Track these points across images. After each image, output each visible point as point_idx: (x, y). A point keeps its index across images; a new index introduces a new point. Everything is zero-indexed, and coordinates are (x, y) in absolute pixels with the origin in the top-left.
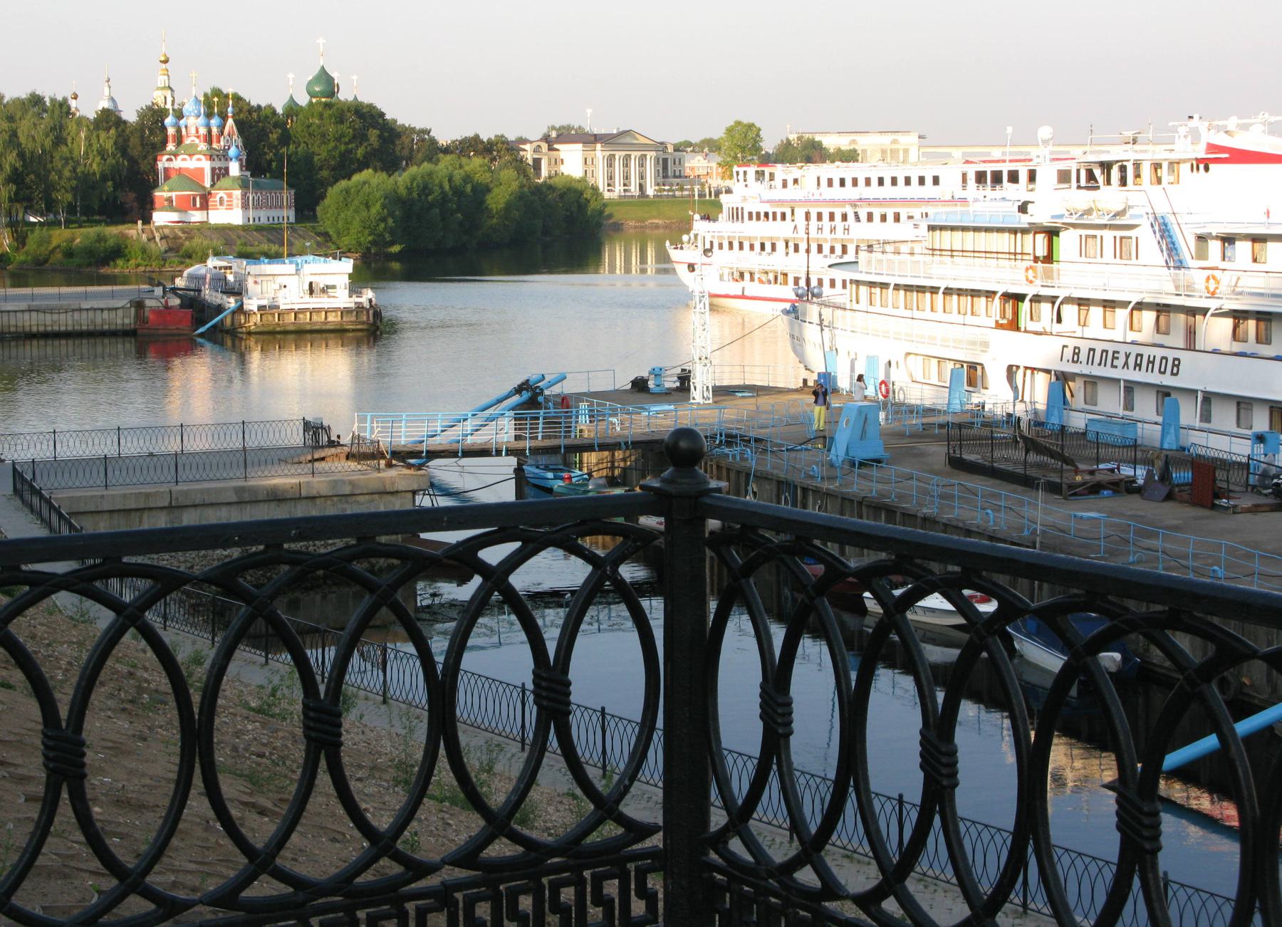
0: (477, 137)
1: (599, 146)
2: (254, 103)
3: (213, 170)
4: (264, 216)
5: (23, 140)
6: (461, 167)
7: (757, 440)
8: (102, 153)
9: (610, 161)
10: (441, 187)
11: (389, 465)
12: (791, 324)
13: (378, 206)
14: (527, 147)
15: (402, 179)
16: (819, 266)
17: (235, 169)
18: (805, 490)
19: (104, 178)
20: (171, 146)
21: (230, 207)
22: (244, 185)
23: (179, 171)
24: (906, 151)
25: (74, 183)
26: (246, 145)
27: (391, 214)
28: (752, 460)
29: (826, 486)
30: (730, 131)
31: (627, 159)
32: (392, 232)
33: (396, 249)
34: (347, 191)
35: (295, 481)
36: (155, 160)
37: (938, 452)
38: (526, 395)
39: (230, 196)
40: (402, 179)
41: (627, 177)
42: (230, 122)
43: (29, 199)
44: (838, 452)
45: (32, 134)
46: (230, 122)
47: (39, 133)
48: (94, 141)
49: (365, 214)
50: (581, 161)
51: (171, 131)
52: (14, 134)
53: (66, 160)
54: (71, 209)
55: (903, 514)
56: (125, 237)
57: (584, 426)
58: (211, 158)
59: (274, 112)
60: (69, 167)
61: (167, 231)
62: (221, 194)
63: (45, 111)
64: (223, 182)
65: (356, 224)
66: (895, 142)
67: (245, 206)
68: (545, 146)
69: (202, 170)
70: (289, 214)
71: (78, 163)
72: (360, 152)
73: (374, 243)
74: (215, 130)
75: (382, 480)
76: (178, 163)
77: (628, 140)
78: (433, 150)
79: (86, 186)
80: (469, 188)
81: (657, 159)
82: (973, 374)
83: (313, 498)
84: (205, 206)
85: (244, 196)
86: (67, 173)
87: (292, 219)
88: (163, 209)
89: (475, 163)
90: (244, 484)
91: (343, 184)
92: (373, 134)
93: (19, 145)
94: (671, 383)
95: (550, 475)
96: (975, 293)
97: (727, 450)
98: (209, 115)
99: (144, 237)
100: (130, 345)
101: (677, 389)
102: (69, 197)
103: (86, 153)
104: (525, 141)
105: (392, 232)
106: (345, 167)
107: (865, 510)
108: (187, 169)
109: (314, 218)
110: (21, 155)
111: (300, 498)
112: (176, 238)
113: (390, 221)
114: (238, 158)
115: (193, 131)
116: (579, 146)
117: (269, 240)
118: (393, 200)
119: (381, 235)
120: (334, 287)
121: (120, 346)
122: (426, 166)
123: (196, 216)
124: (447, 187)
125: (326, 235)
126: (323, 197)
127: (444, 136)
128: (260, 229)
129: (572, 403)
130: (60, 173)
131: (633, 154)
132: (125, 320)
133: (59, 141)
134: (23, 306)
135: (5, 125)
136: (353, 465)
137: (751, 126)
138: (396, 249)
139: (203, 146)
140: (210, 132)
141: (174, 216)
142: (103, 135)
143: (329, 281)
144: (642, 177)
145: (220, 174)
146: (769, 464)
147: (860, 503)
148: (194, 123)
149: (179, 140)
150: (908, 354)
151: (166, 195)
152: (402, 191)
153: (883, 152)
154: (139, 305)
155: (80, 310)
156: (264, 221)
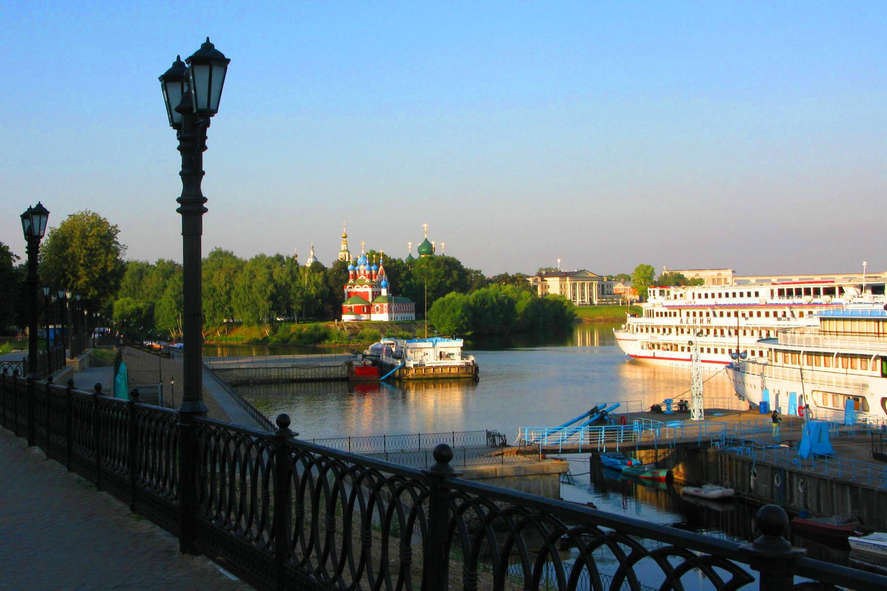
1: (568, 278)
3: (373, 293)
4: (399, 317)
5: (275, 277)
7: (746, 442)
8: (316, 284)
9: (574, 286)
10: (492, 300)
11: (544, 458)
12: (735, 375)
13: (460, 311)
14: (530, 279)
16: (748, 342)
17: (384, 292)
18: (790, 473)
19: (317, 297)
20: (351, 281)
21: (382, 312)
22: (389, 301)
23: (356, 293)
24: (725, 279)
25: (302, 300)
27: (467, 315)
28: (753, 455)
29: (806, 471)
30: (637, 269)
31: (582, 286)
32: (467, 324)
34: (443, 303)
35: (493, 467)
36: (343, 288)
37: (865, 452)
38: (596, 416)
39: (382, 306)
41: (583, 295)
42: (381, 267)
43: (279, 309)
44: (804, 449)
45: (280, 274)
46: (381, 267)
47: (284, 275)
48: (312, 278)
49: (452, 315)
51: (351, 273)
52: (271, 275)
54: (300, 314)
55: (863, 489)
56: (329, 328)
57: (640, 435)
58: (372, 286)
61: (350, 325)
62: (377, 305)
63: (284, 263)
64: (379, 299)
65: (448, 321)
67: (390, 311)
68: (539, 279)
70: (413, 315)
71: (303, 290)
72: (448, 282)
74: (374, 272)
75: (542, 467)
77: (583, 275)
78: (485, 282)
79: (308, 301)
80: (506, 301)
81: (599, 285)
82: (857, 403)
83: (503, 477)
85: (389, 306)
86: (298, 295)
87: (414, 318)
88: (347, 313)
90: (464, 469)
91: (441, 299)
92: (455, 273)
93: (274, 281)
94: (674, 408)
95: (619, 462)
96: (853, 356)
97: (734, 448)
98: (370, 264)
99: (339, 328)
100: (344, 386)
101: (678, 411)
102: (299, 307)
103: (308, 284)
104: (529, 277)
105: (467, 324)
106: (440, 291)
107: (834, 486)
108: (360, 293)
110: (275, 286)
111: (496, 477)
112: (355, 328)
113: (466, 319)
114: (386, 287)
115: (362, 272)
116: (558, 279)
117: (404, 330)
118: (467, 307)
119: (461, 326)
120: (453, 354)
121: (340, 387)
124: (495, 300)
127: (489, 274)
128: (398, 323)
129: (628, 421)
130: (295, 295)
131: (586, 283)
132: (344, 373)
134: (289, 364)
135: (267, 271)
136: (521, 458)
137: (649, 267)
139: (368, 281)
141: (352, 317)
142: (317, 275)
143: (451, 351)
144: (591, 294)
145: (377, 294)
146: (763, 456)
147: (831, 482)
148: (363, 268)
149: (355, 277)
150: (813, 391)
151: (348, 306)
152: (471, 302)
153: (713, 280)
154: (350, 364)
155: (319, 367)
156: (399, 319)
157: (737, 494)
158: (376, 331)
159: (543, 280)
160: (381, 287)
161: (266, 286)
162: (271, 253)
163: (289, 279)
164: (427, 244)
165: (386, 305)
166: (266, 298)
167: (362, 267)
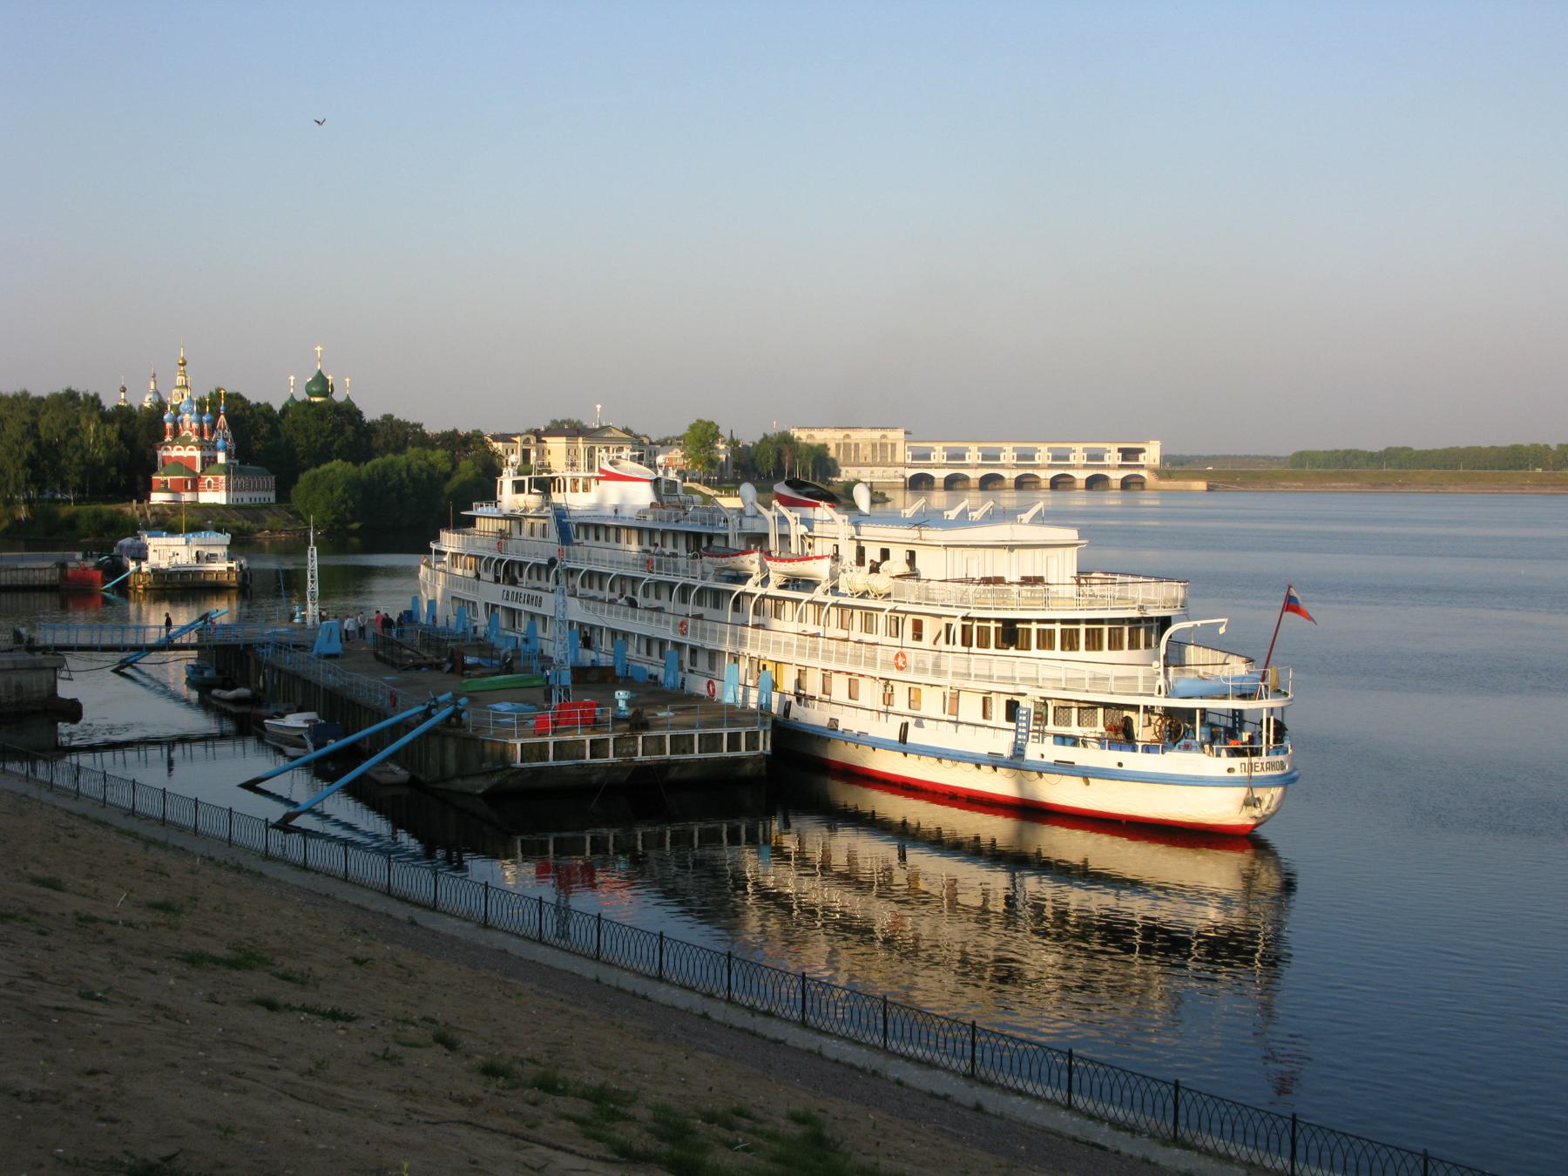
0: (455, 431)
2: (253, 402)
3: (203, 458)
4: (246, 498)
5: (42, 432)
6: (426, 458)
8: (107, 443)
14: (518, 439)
15: (365, 469)
17: (221, 458)
20: (168, 438)
21: (216, 490)
22: (226, 470)
24: (894, 445)
26: (235, 439)
30: (692, 427)
33: (356, 525)
34: (315, 477)
40: (365, 469)
50: (564, 452)
51: (169, 425)
52: (35, 425)
53: (77, 448)
54: (80, 489)
56: (121, 513)
58: (201, 448)
59: (269, 408)
60: (79, 454)
62: (209, 478)
64: (212, 468)
66: (847, 436)
67: (228, 490)
68: (533, 440)
69: (194, 458)
70: (272, 496)
73: (336, 521)
76: (175, 452)
79: (92, 470)
80: (424, 476)
84: (195, 489)
85: (228, 481)
86: (76, 460)
87: (273, 500)
89: (439, 456)
91: (313, 471)
92: (349, 429)
93: (39, 437)
98: (201, 413)
100: (48, 600)
102: (78, 480)
104: (516, 435)
106: (323, 456)
109: (288, 499)
110: (38, 445)
112: (165, 514)
113: (350, 503)
114: (225, 449)
116: (564, 439)
118: (355, 484)
122: (390, 457)
123: (187, 497)
124: (404, 475)
125: (297, 514)
126: (295, 481)
127: (432, 428)
133: (72, 433)
135: (28, 419)
137: (710, 424)
138: (356, 525)
139: (195, 439)
140: (201, 426)
142: (109, 428)
143: (213, 551)
145: (209, 462)
148: (189, 420)
149: (176, 432)
153: (874, 446)
156: (246, 501)
157: (253, 694)
158: (197, 519)
159: (539, 441)
160: (216, 450)
161: (21, 444)
162: (42, 387)
163: (63, 434)
164: (321, 379)
165: (223, 478)
166: (19, 463)
167: (187, 416)
